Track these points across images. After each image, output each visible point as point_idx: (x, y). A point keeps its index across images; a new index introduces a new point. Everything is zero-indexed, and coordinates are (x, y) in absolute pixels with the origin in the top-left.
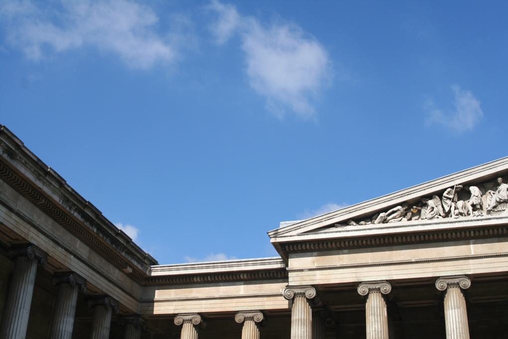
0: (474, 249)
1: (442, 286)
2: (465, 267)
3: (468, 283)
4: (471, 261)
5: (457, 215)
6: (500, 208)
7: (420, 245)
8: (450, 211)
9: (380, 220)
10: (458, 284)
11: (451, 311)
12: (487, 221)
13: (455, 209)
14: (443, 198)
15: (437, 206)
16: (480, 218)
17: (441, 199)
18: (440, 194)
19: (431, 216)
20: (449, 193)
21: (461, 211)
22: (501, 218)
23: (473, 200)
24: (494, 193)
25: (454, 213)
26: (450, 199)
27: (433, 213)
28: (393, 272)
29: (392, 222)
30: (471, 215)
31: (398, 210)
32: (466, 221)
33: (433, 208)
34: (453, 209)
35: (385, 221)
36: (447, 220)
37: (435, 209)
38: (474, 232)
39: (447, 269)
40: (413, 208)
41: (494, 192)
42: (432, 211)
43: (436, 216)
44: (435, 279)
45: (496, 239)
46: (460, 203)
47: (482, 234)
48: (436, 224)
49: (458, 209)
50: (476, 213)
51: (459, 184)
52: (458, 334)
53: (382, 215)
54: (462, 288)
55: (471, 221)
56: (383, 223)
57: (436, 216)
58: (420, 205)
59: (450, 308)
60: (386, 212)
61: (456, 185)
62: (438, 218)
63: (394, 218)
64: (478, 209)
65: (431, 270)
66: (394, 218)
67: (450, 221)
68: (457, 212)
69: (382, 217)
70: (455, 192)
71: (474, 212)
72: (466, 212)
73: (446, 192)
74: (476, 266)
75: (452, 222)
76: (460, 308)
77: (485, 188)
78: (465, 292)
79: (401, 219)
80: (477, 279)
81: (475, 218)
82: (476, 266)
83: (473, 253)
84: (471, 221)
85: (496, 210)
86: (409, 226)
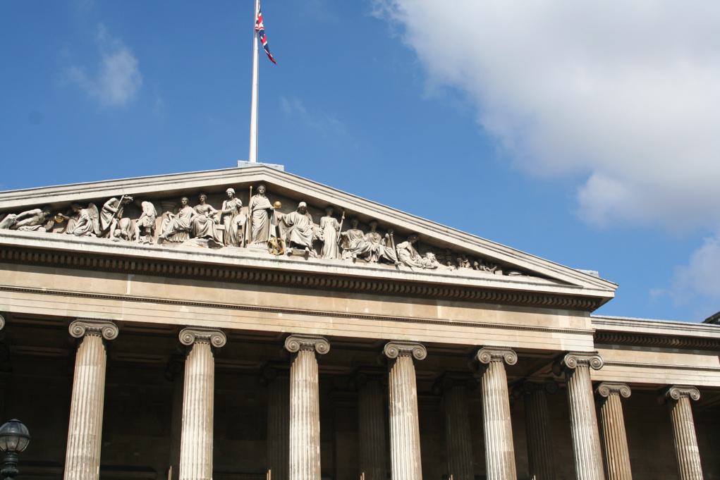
0: (131, 287)
1: (78, 332)
2: (114, 310)
3: (114, 332)
4: (124, 302)
5: (117, 237)
6: (177, 238)
7: (57, 269)
8: (108, 229)
9: (4, 224)
10: (101, 331)
11: (84, 367)
12: (156, 252)
13: (116, 228)
14: (103, 209)
15: (91, 219)
16: (147, 246)
17: (100, 210)
18: (99, 203)
19: (81, 232)
20: (112, 204)
21: (124, 232)
22: (176, 252)
23: (143, 220)
24: (173, 217)
25: (114, 233)
26: (112, 213)
27: (84, 227)
28: (12, 302)
29: (23, 229)
30: (137, 240)
31: (36, 214)
32: (128, 247)
33: (86, 221)
34: (113, 227)
35: (13, 226)
37: (89, 223)
38: (136, 264)
39: (90, 308)
40: (57, 216)
41: (173, 215)
42: (85, 224)
43: (88, 233)
44: (70, 320)
45: (164, 278)
46: (125, 222)
47: (146, 268)
48: (86, 243)
49: (120, 228)
50: (144, 238)
51: (129, 195)
52: (89, 401)
53: (10, 216)
54: (106, 338)
55: (135, 248)
56: (10, 228)
57: (88, 233)
58: (68, 213)
59: (84, 364)
60: (17, 214)
61: (125, 196)
62: (90, 236)
63: (27, 224)
64: (148, 233)
65: (66, 306)
66: (27, 224)
67: (106, 243)
68: (118, 232)
69: (9, 220)
70: (121, 204)
71: (141, 237)
72: (130, 235)
73: (109, 202)
74: (130, 311)
75: (108, 246)
76: (97, 364)
77: (162, 207)
78: (108, 344)
79: (38, 228)
80: (127, 328)
81: (141, 245)
82: (130, 311)
83: (128, 293)
84: (135, 248)
85: (171, 240)
86: (47, 240)
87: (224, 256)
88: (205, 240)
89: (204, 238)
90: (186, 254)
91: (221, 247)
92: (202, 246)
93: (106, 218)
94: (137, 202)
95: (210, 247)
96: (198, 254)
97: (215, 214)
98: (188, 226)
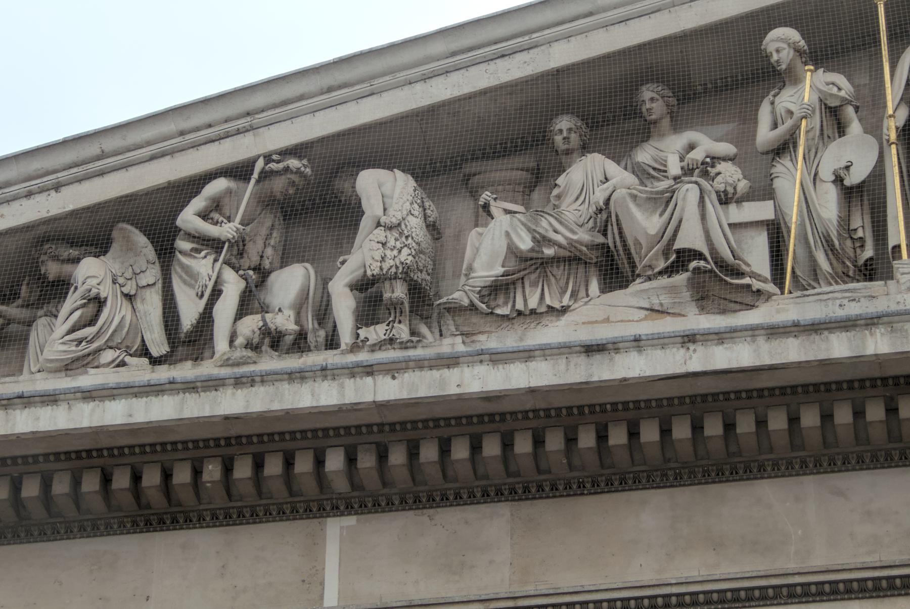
8: (206, 319)
14: (183, 245)
15: (129, 297)
19: (74, 351)
26: (214, 245)
33: (99, 302)
36: (185, 371)
42: (92, 322)
48: (88, 395)
57: (108, 356)
61: (268, 158)
62: (123, 364)
64: (395, 306)
68: (250, 324)
70: (266, 202)
73: (198, 203)
87: (774, 331)
88: (681, 278)
89: (670, 271)
90: (582, 359)
91: (769, 296)
92: (656, 312)
93: (191, 276)
94: (342, 184)
95: (702, 309)
96: (638, 343)
97: (715, 159)
98: (584, 236)
